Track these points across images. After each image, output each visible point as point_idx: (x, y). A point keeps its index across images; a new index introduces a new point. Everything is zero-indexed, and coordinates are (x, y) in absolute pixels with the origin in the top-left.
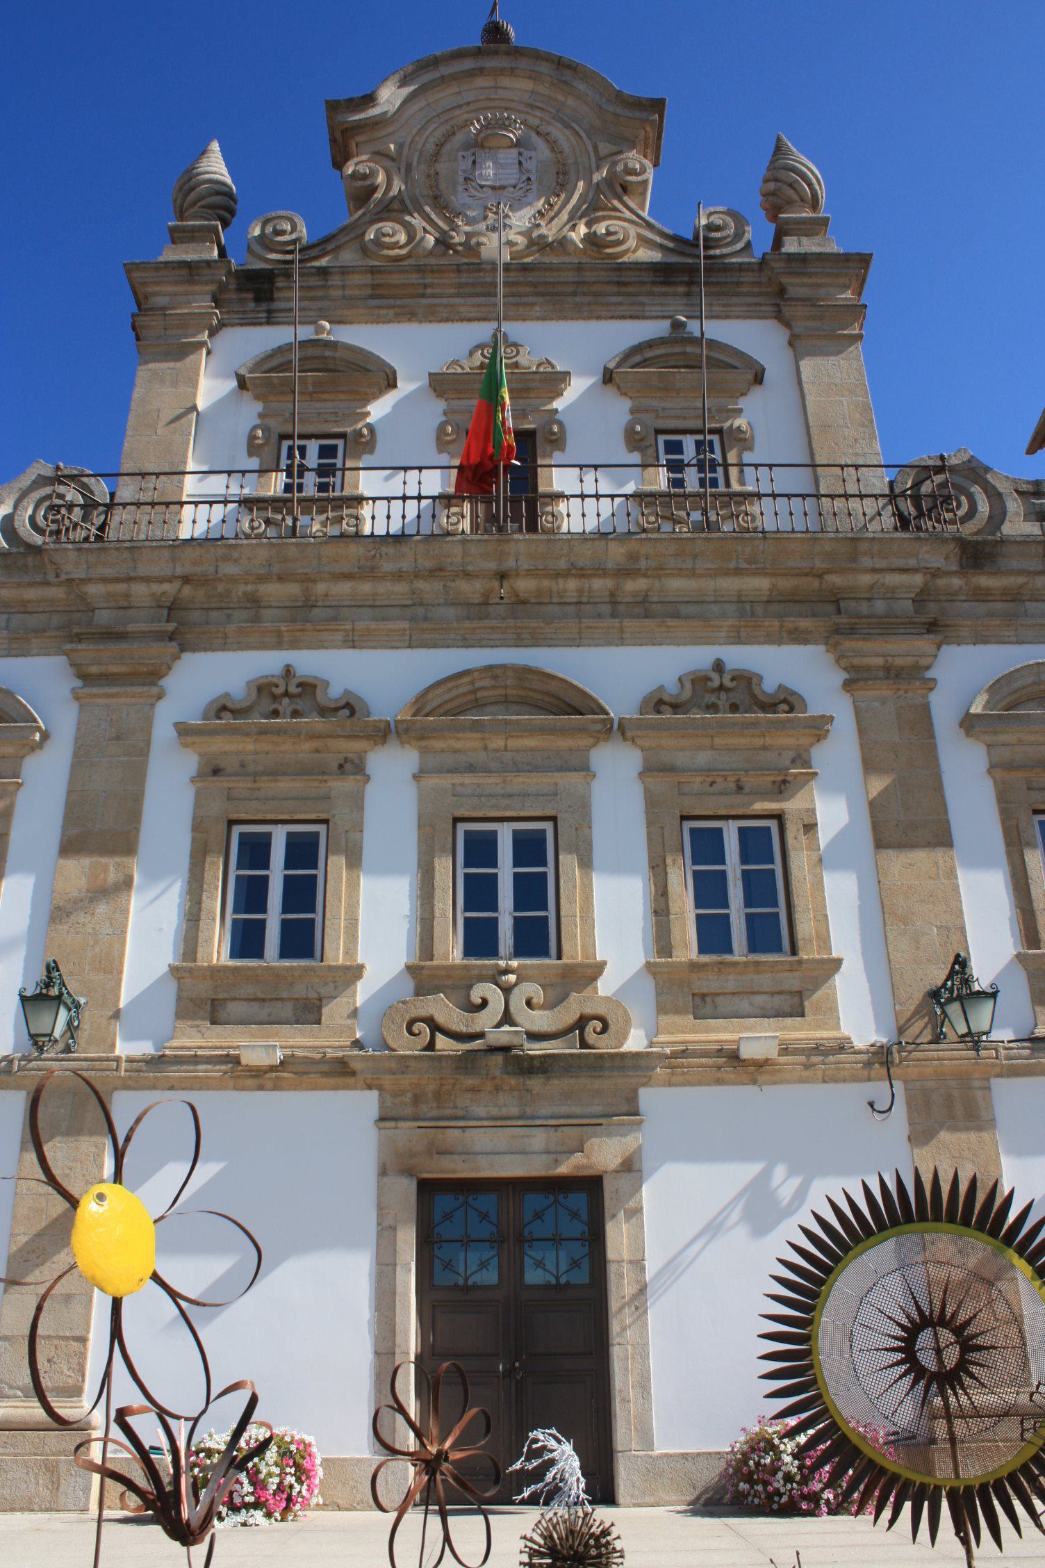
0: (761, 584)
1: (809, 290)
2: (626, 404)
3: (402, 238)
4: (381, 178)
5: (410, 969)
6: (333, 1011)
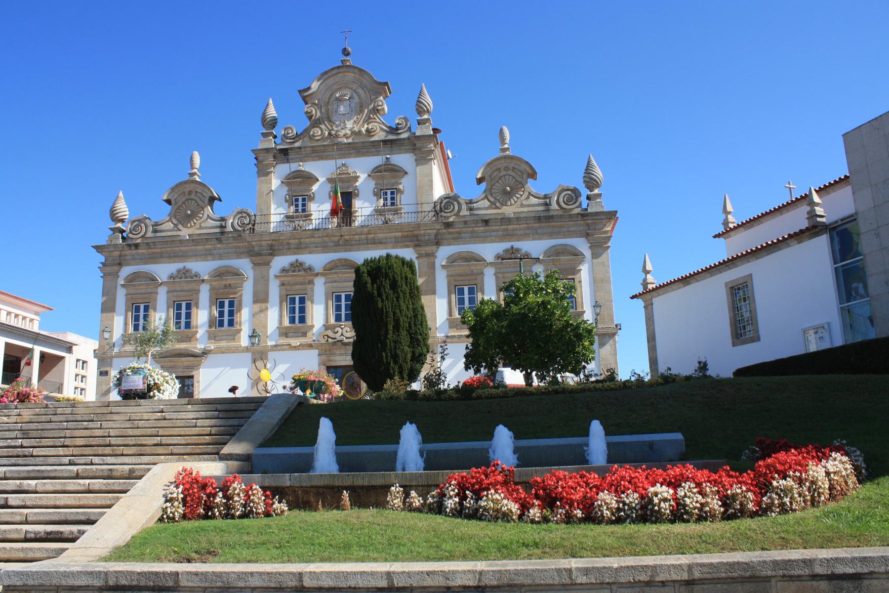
0: (399, 234)
1: (420, 147)
2: (374, 182)
3: (320, 133)
4: (314, 112)
5: (324, 325)
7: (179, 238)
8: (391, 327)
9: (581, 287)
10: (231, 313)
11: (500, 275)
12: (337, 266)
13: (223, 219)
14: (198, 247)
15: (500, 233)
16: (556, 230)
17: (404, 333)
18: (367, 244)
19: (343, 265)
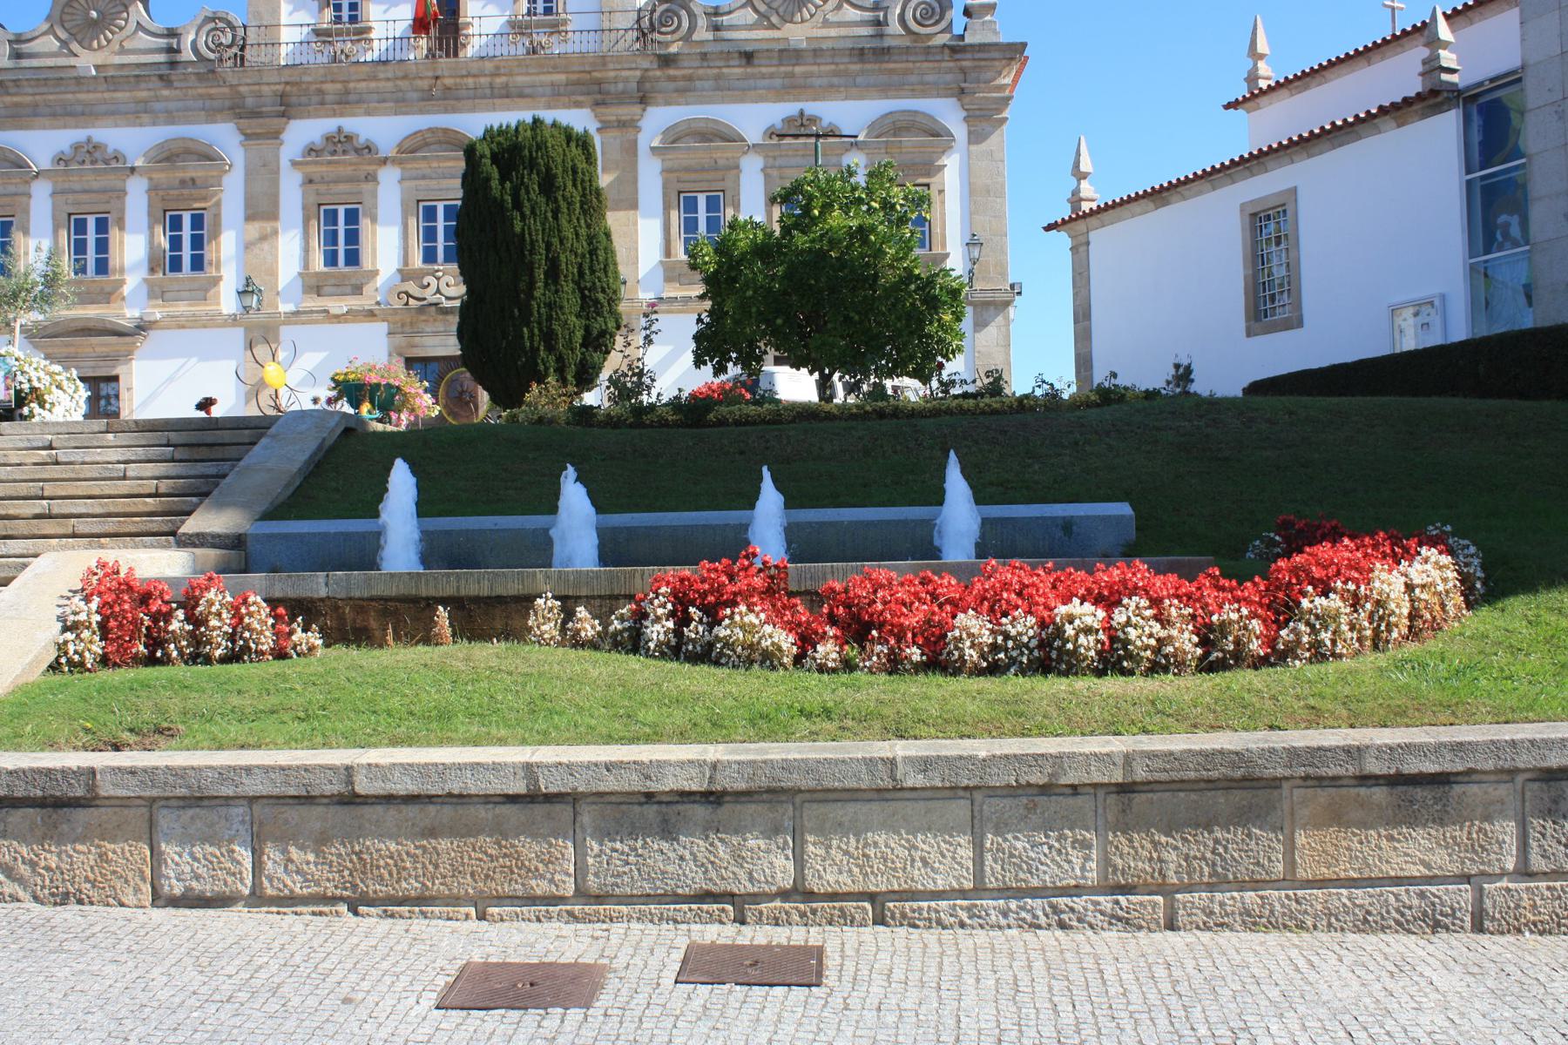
0: (563, 77)
6: (367, 289)
7: (74, 74)
8: (540, 275)
9: (943, 202)
10: (197, 242)
11: (775, 173)
12: (427, 144)
13: (172, 33)
14: (119, 95)
15: (778, 82)
16: (896, 78)
17: (568, 287)
18: (493, 96)
19: (440, 142)
